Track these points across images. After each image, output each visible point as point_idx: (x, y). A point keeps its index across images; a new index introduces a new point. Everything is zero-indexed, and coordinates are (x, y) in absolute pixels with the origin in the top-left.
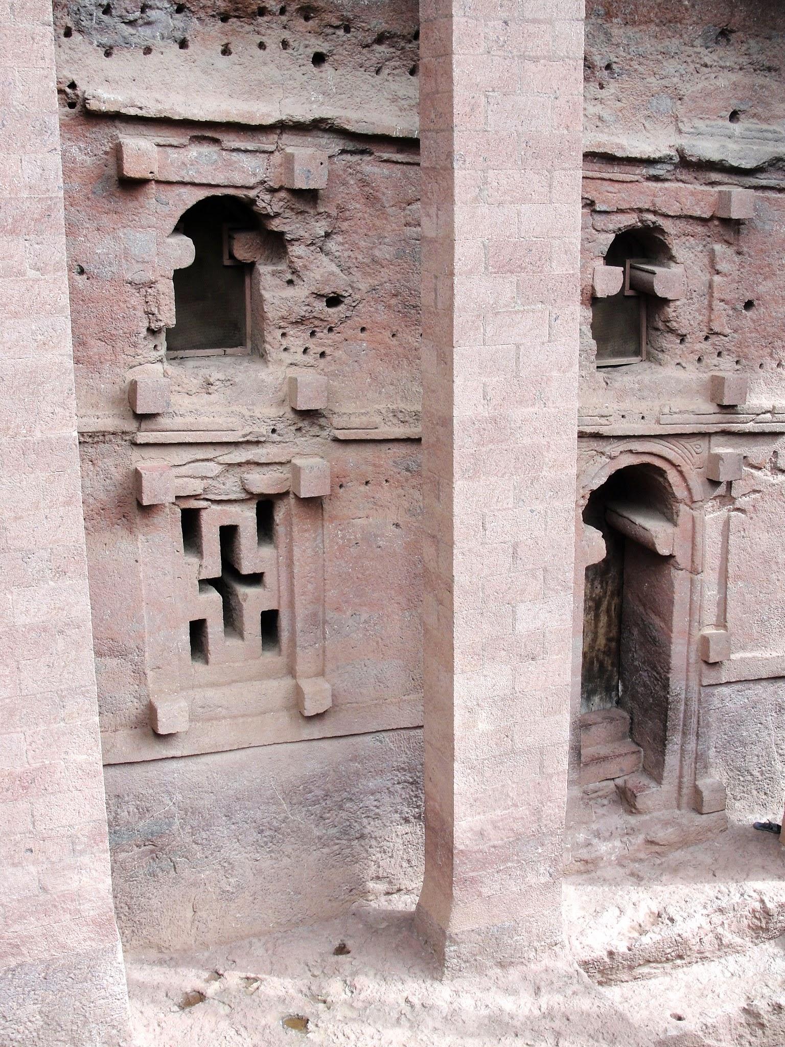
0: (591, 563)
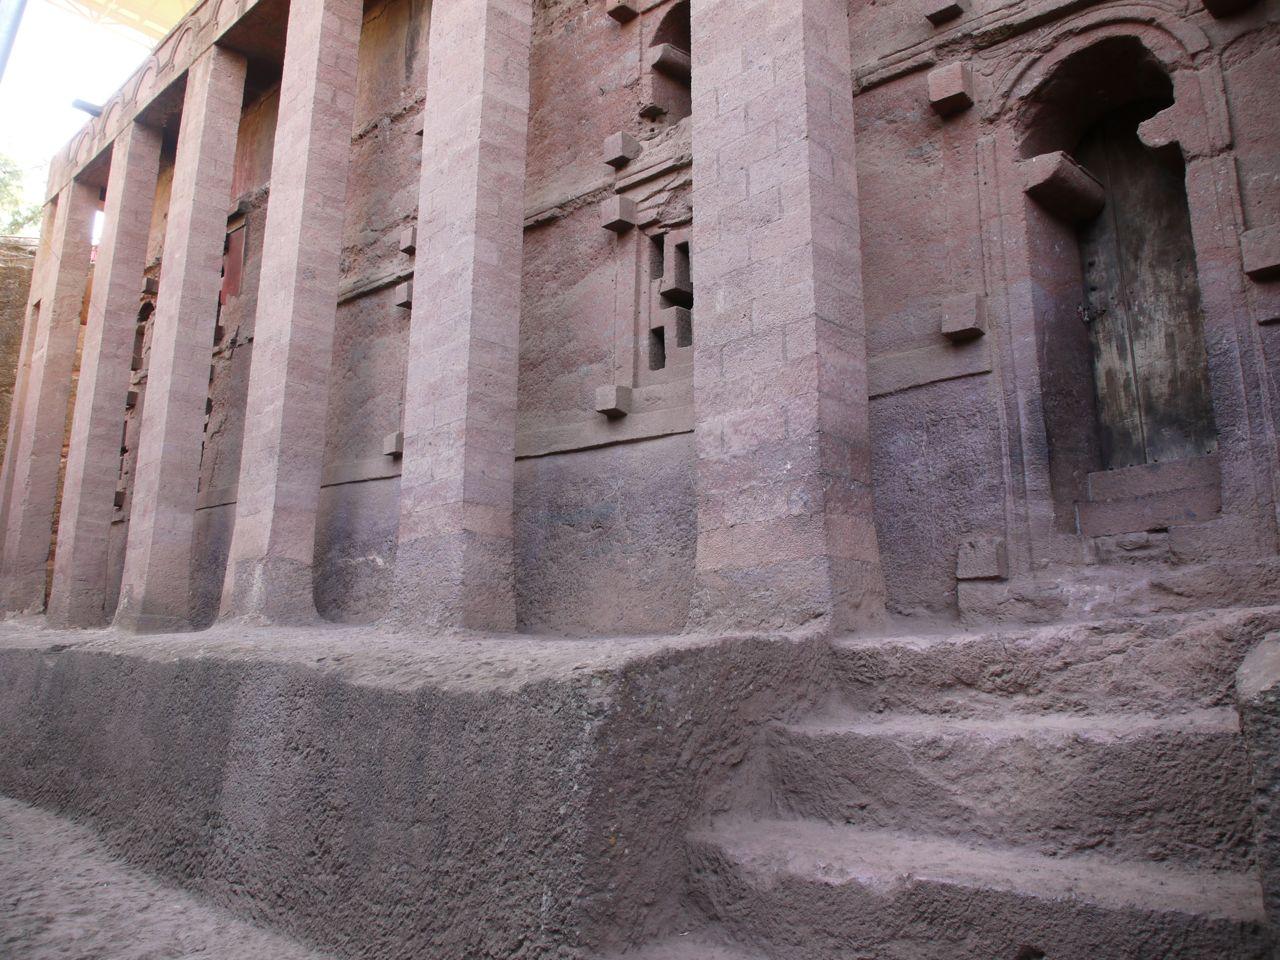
0: (1032, 184)
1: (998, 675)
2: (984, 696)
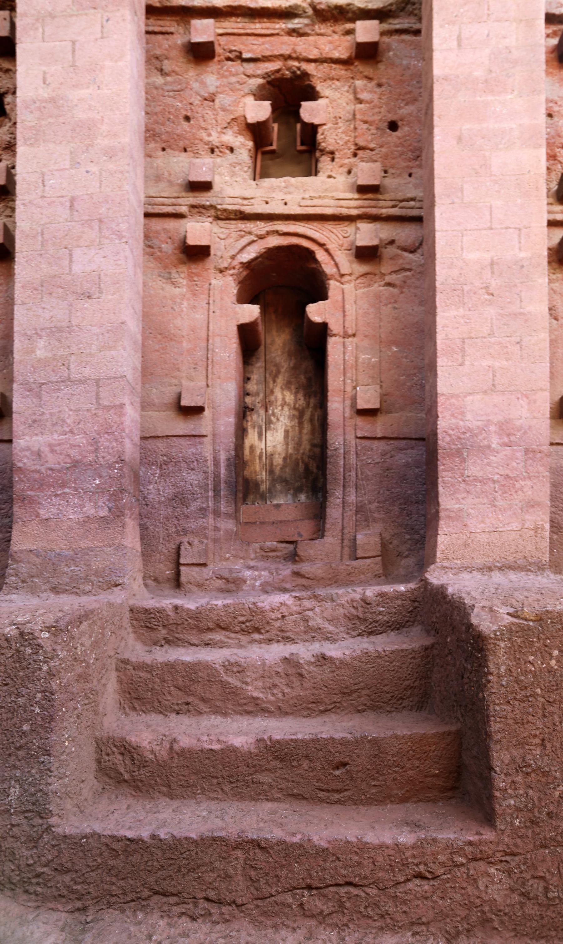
1: (243, 623)
2: (233, 635)
